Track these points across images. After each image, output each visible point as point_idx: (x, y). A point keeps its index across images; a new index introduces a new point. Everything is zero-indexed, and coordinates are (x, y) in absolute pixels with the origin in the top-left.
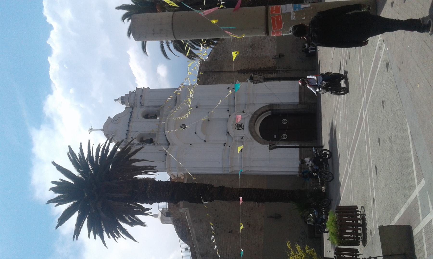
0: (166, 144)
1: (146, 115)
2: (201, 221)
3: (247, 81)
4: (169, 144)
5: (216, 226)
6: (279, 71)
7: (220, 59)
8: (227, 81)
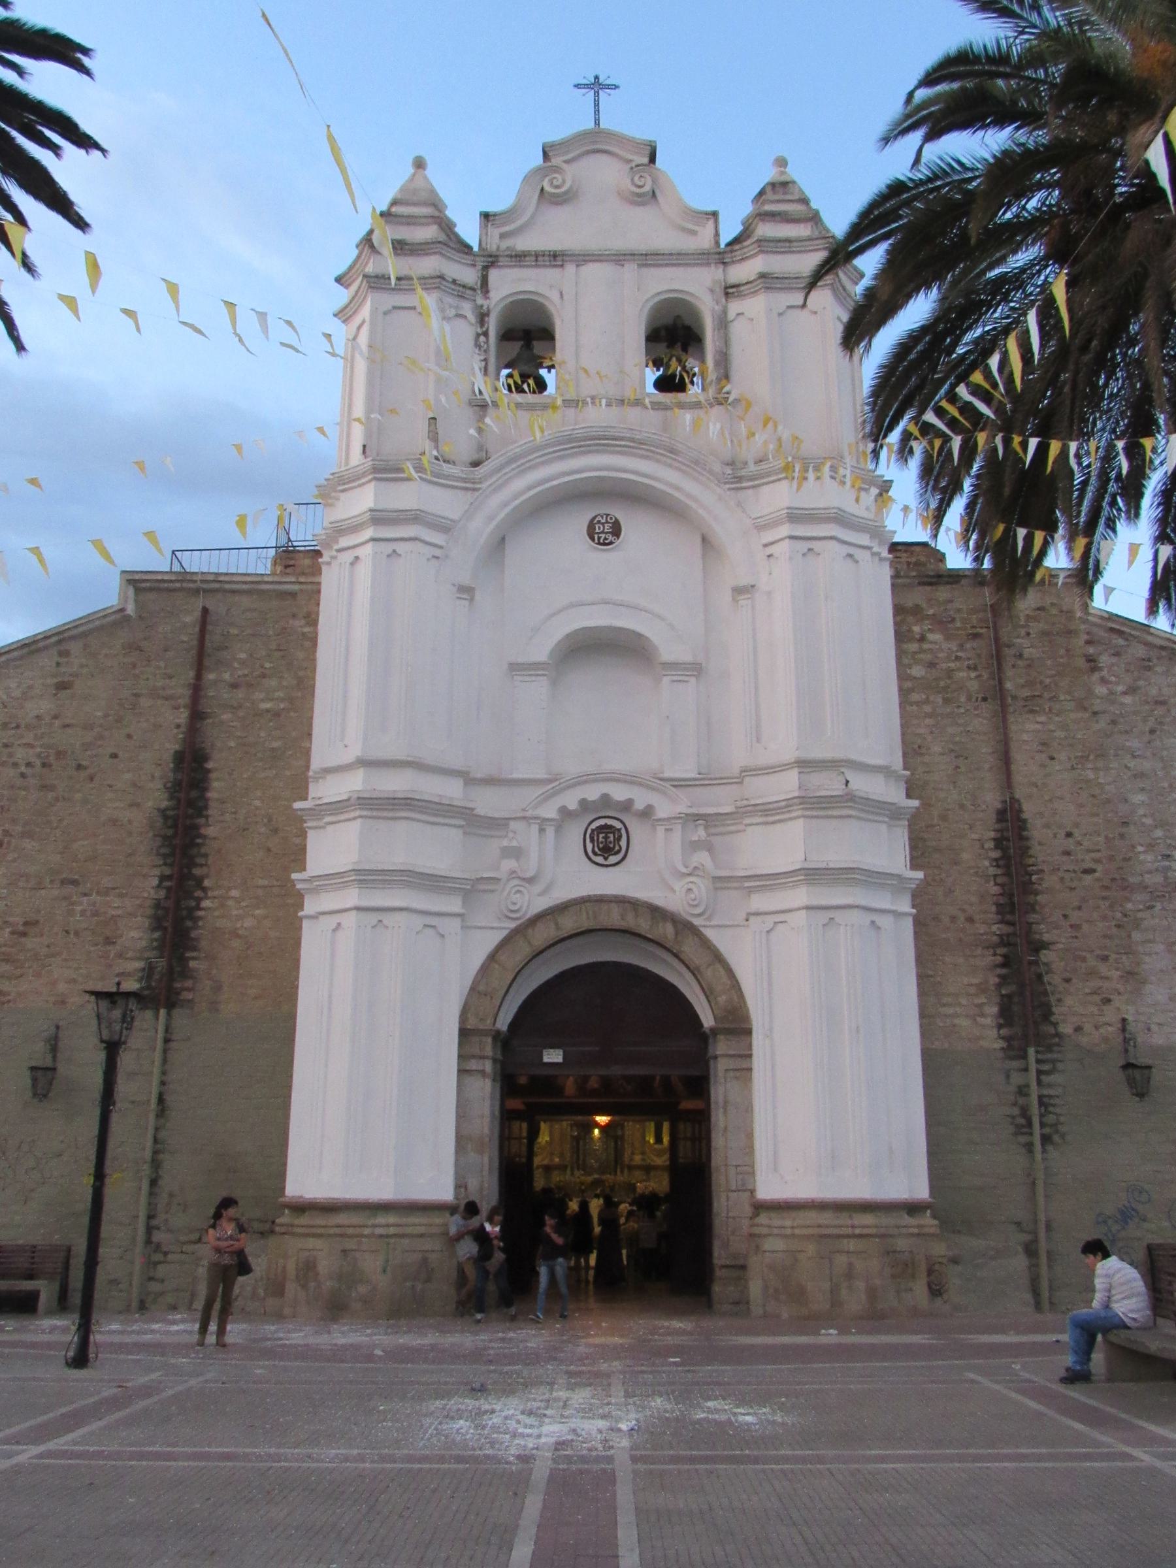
0: (480, 447)
1: (688, 329)
2: (62, 686)
3: (914, 866)
4: (476, 464)
5: (29, 765)
6: (1026, 1070)
7: (1101, 690)
8: (937, 749)
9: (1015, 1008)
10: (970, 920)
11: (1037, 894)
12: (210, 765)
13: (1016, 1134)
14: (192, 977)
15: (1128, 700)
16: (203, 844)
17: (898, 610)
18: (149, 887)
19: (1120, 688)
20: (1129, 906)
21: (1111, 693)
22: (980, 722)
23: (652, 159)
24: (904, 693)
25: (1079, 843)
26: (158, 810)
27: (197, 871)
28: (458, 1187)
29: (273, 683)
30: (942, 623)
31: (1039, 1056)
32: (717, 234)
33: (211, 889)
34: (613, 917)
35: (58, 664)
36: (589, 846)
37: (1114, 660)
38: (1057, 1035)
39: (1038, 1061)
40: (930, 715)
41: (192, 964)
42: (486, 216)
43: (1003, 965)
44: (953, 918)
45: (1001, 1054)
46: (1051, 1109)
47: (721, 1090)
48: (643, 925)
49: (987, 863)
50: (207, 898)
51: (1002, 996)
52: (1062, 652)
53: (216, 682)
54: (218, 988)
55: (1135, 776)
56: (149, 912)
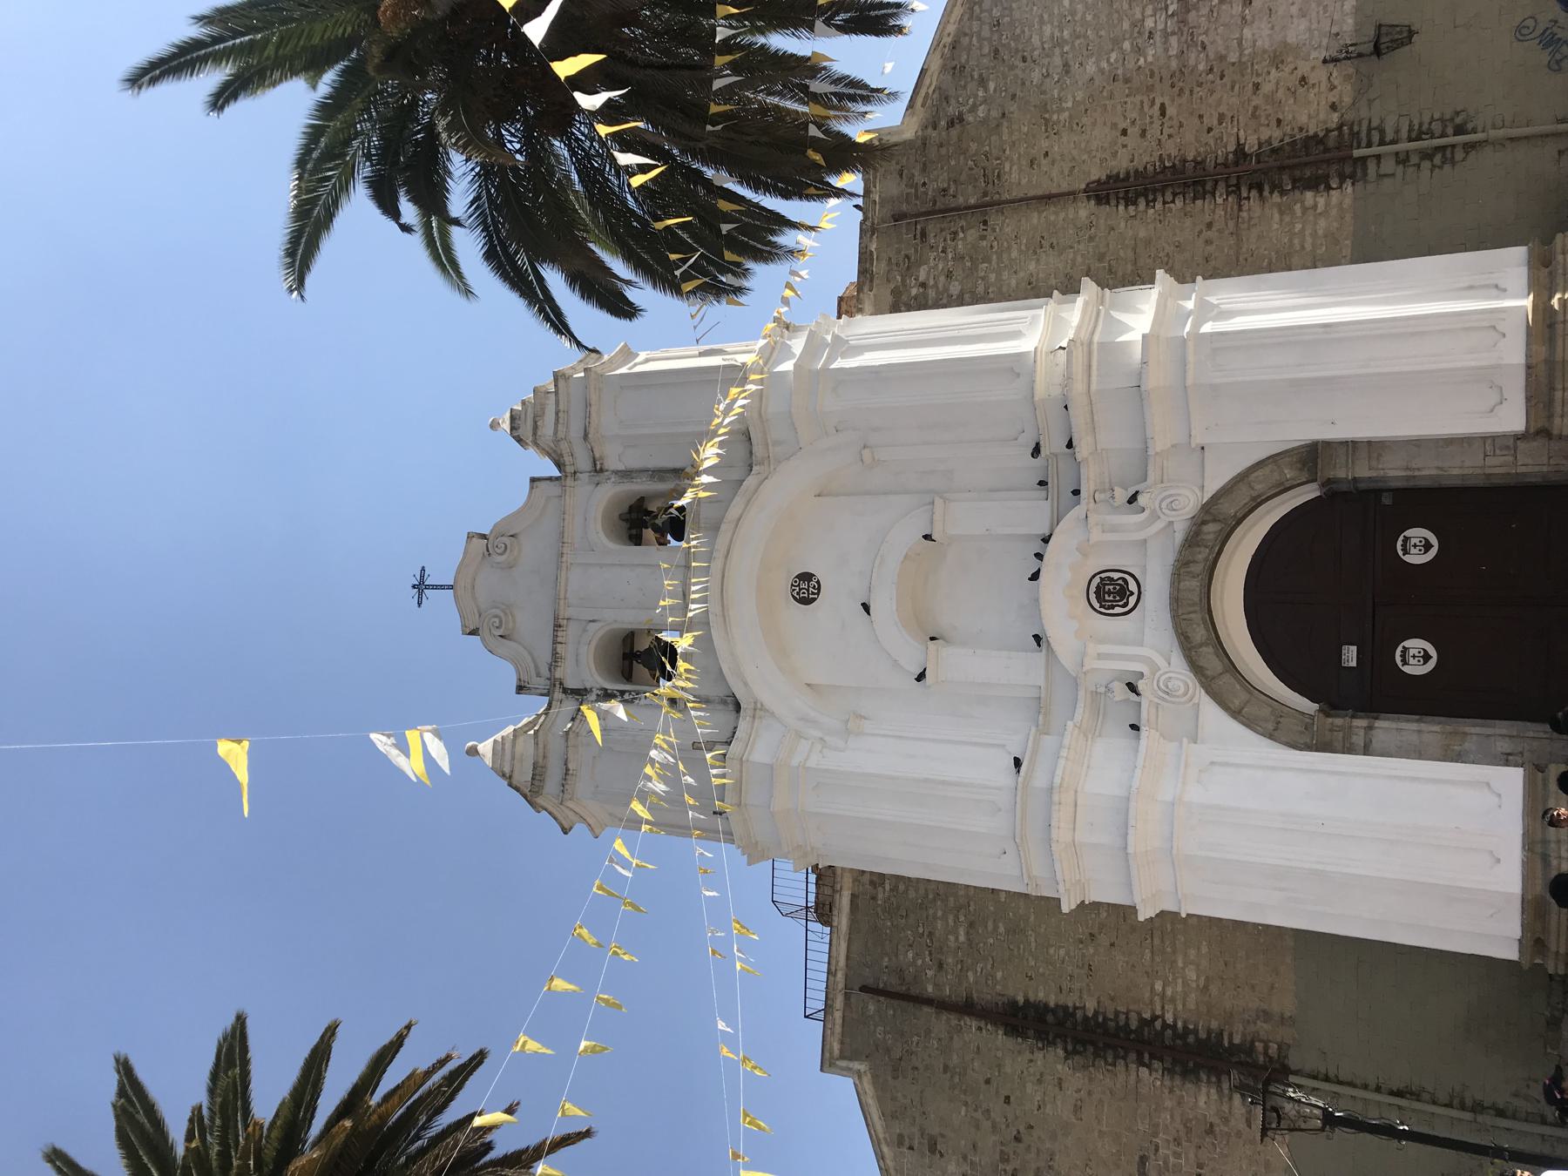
0: (724, 702)
2: (933, 1148)
4: (738, 707)
6: (1378, 157)
8: (1032, 266)
9: (1308, 174)
10: (1210, 225)
11: (1185, 161)
12: (1021, 999)
13: (1453, 163)
14: (1252, 1042)
15: (992, 86)
16: (1104, 1014)
17: (895, 308)
18: (1149, 1079)
19: (981, 94)
20: (1201, 67)
21: (985, 101)
22: (1006, 225)
23: (484, 536)
24: (976, 300)
25: (1133, 122)
26: (1066, 1058)
27: (1134, 1025)
28: (1507, 764)
29: (939, 924)
30: (909, 266)
31: (1364, 143)
32: (550, 479)
33: (1153, 1011)
34: (1194, 584)
35: (911, 1148)
36: (1118, 610)
37: (953, 101)
38: (1340, 128)
39: (1369, 145)
40: (999, 274)
41: (1237, 1040)
42: (520, 689)
43: (1261, 191)
44: (1208, 242)
45: (1359, 185)
46: (1425, 127)
47: (1391, 473)
48: (1202, 554)
49: (1151, 211)
50: (1163, 1017)
51: (1293, 188)
52: (943, 151)
53: (935, 985)
54: (1266, 1015)
55: (1067, 72)
56: (1178, 1081)
